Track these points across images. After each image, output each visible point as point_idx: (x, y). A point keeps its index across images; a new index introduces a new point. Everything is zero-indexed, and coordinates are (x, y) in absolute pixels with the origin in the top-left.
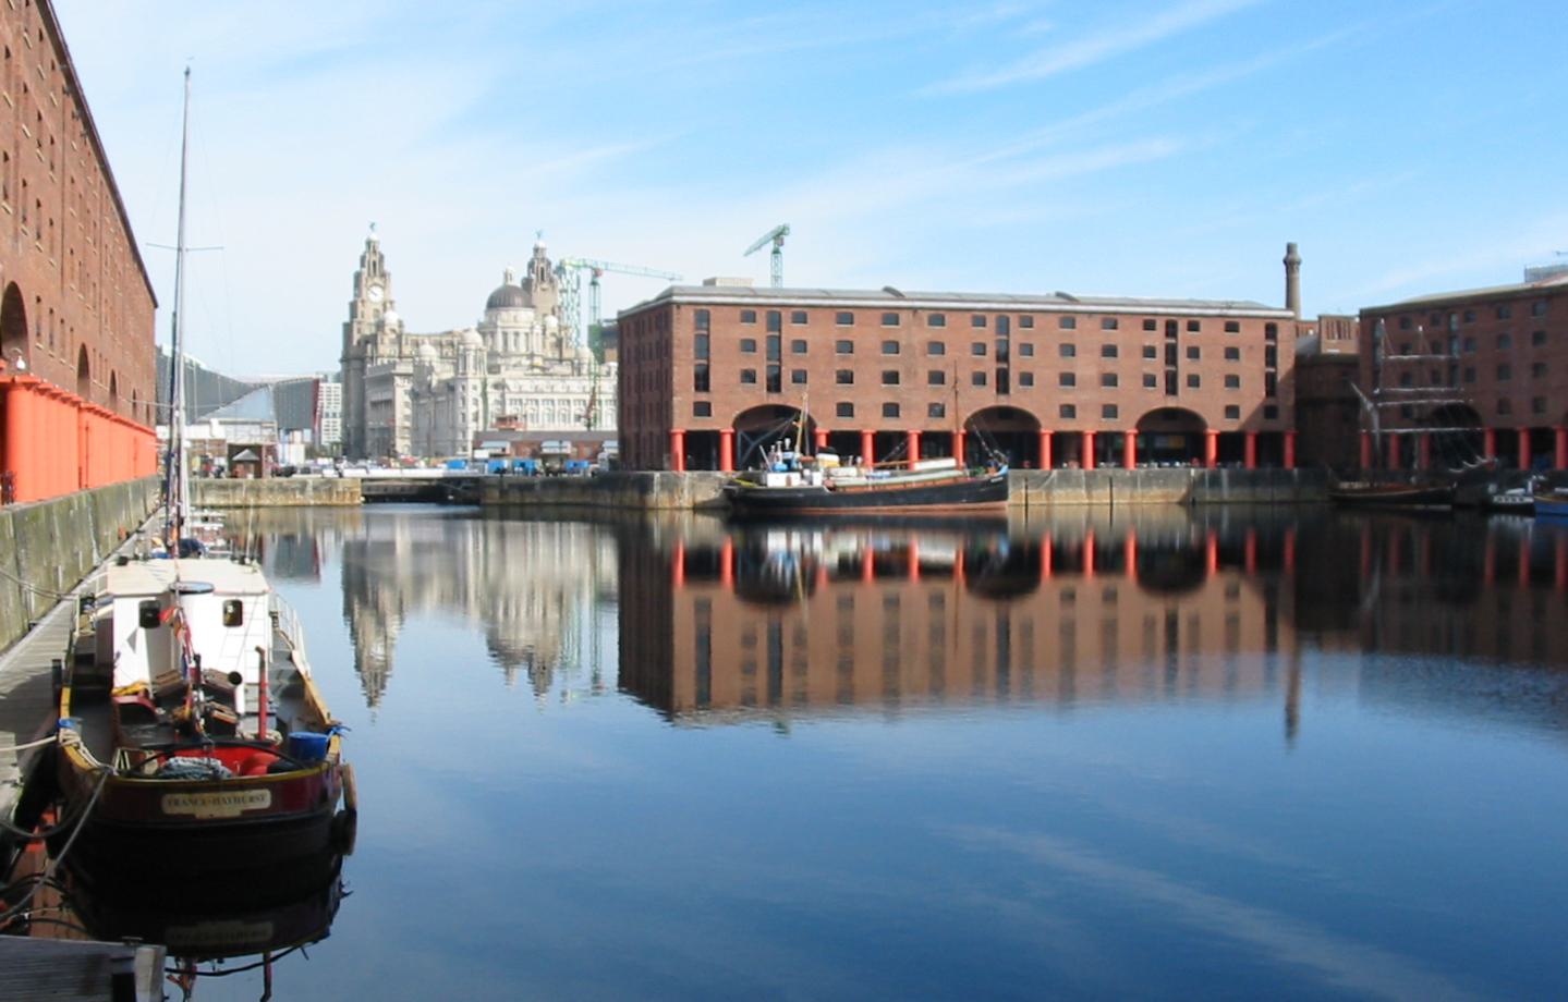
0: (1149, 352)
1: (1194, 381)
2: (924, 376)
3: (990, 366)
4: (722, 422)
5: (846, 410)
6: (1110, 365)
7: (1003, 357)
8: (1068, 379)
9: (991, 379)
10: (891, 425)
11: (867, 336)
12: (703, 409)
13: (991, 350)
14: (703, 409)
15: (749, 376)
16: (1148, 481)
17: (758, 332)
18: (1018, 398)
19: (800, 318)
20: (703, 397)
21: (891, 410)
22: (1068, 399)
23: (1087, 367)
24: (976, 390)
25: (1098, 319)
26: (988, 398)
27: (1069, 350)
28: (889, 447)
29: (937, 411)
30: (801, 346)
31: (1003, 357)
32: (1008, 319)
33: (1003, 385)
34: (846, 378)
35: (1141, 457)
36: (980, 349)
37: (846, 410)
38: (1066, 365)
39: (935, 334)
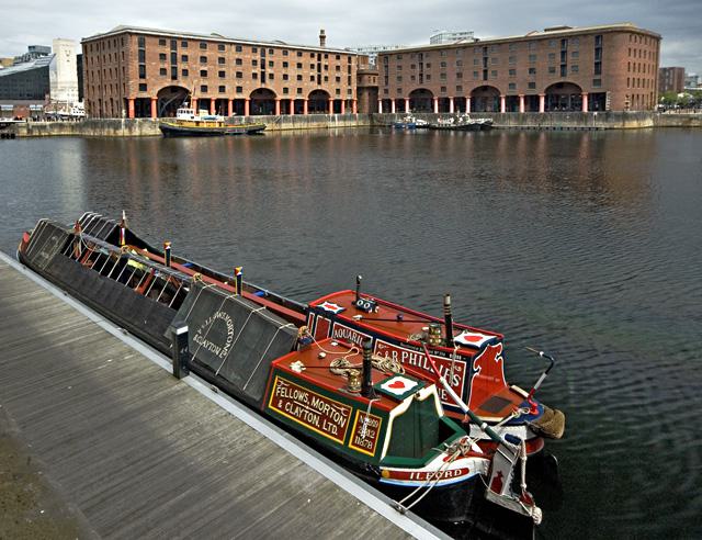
0: (312, 66)
1: (326, 78)
3: (258, 70)
4: (152, 93)
7: (263, 67)
10: (222, 96)
12: (143, 87)
13: (259, 63)
14: (143, 87)
15: (163, 71)
16: (313, 120)
19: (185, 45)
20: (143, 81)
22: (286, 85)
24: (253, 81)
28: (221, 106)
29: (239, 89)
30: (185, 58)
31: (263, 67)
33: (263, 81)
35: (310, 110)
36: (255, 62)
37: (204, 89)
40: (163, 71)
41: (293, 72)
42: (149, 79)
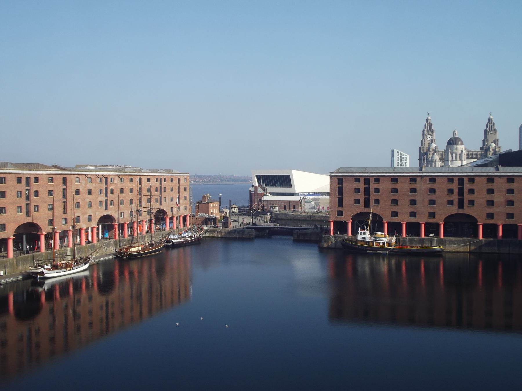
2: (427, 202)
3: (455, 197)
5: (395, 214)
6: (510, 197)
8: (491, 203)
9: (456, 202)
11: (404, 186)
12: (340, 213)
14: (340, 213)
15: (357, 202)
17: (361, 186)
18: (467, 210)
20: (340, 209)
21: (413, 214)
22: (490, 211)
23: (499, 198)
24: (448, 207)
25: (505, 178)
26: (454, 210)
27: (491, 191)
30: (377, 191)
32: (463, 179)
34: (395, 202)
36: (451, 191)
38: (489, 197)
39: (431, 185)
40: (357, 202)
41: (499, 198)
42: (345, 209)
